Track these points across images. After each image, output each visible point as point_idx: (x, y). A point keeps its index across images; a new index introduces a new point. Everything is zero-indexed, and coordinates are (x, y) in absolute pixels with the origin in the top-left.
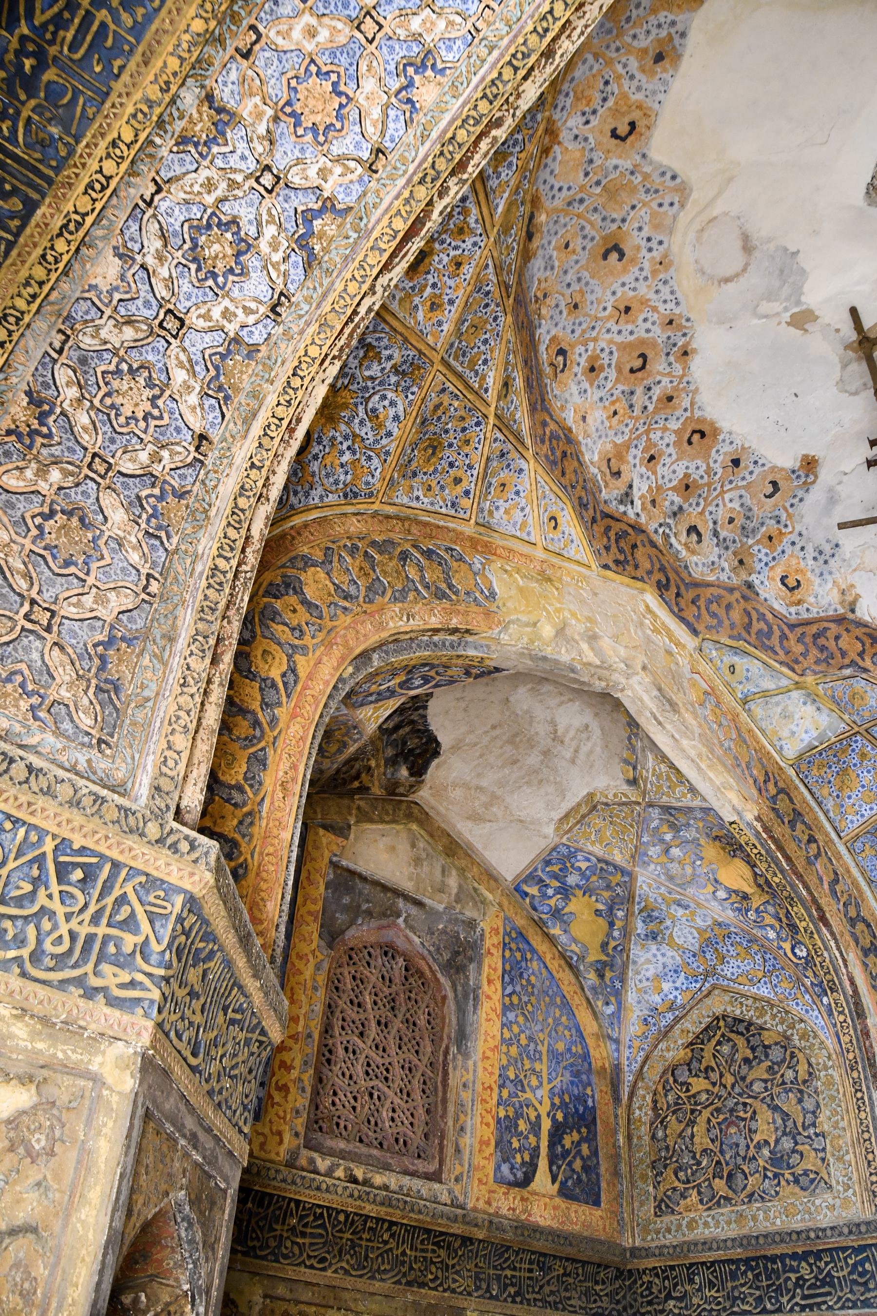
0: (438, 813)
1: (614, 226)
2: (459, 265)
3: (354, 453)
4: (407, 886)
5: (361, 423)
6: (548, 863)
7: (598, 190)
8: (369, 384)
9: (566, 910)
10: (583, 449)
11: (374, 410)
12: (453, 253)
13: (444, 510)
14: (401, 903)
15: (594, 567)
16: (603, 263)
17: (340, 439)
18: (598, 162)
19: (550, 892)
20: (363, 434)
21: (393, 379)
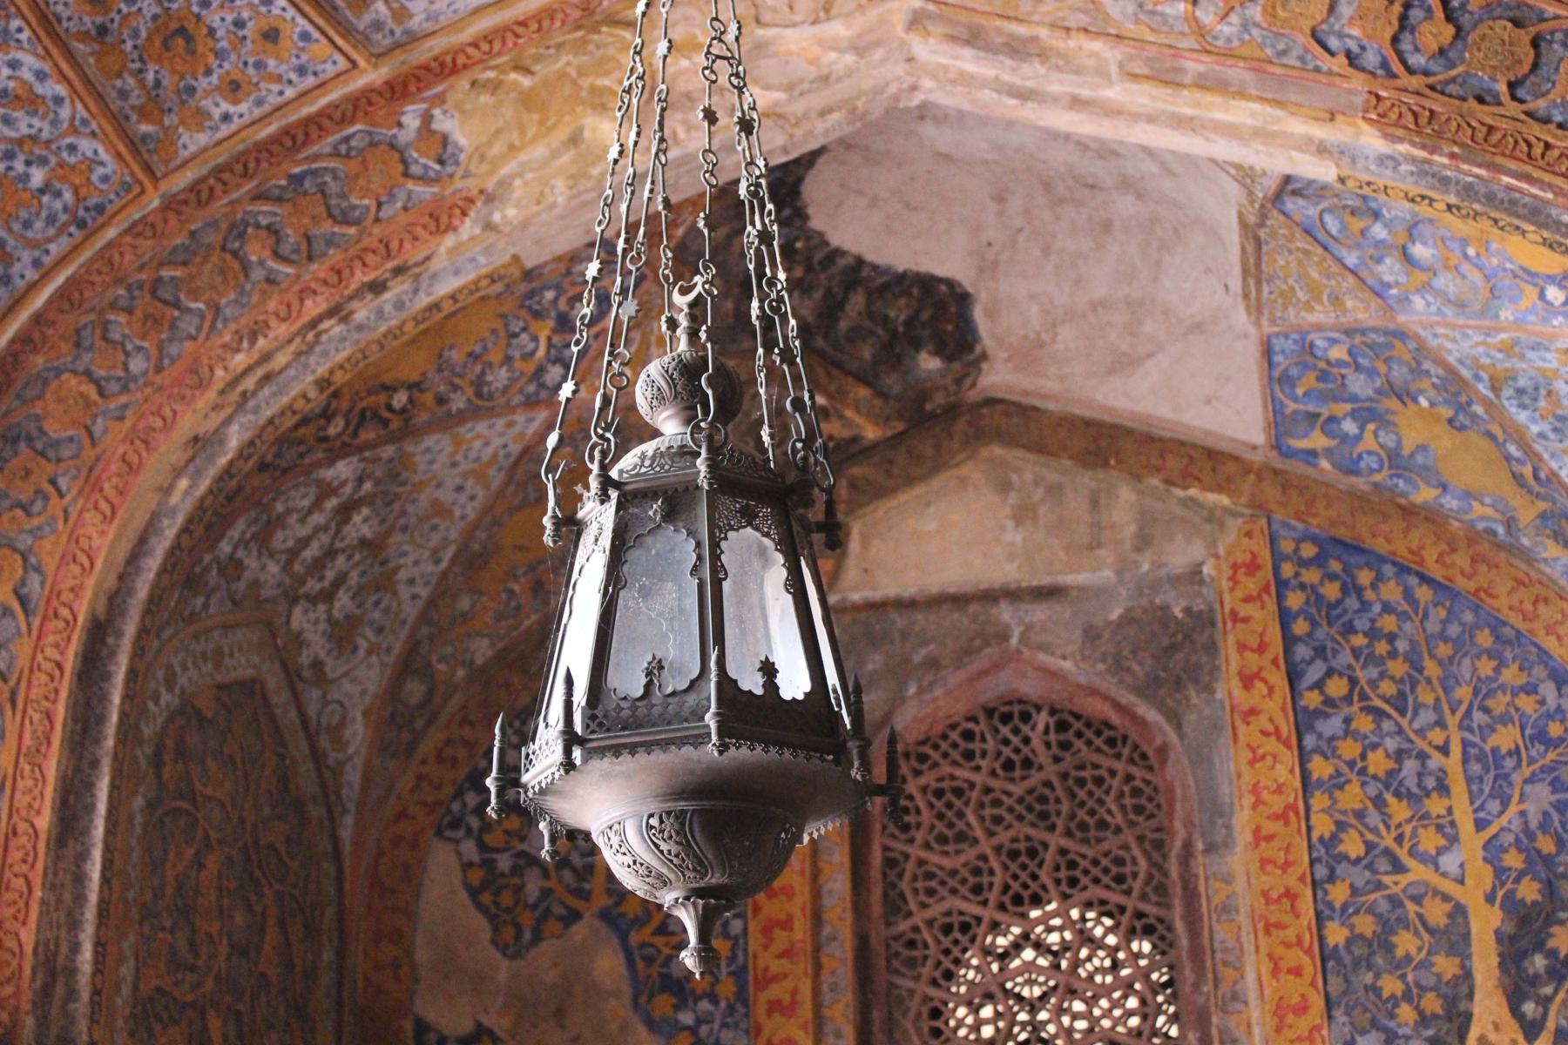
0: (1045, 397)
3: (43, 161)
4: (1008, 573)
6: (1286, 380)
9: (1406, 452)
13: (290, 93)
14: (1005, 612)
19: (1350, 427)
20: (25, 131)
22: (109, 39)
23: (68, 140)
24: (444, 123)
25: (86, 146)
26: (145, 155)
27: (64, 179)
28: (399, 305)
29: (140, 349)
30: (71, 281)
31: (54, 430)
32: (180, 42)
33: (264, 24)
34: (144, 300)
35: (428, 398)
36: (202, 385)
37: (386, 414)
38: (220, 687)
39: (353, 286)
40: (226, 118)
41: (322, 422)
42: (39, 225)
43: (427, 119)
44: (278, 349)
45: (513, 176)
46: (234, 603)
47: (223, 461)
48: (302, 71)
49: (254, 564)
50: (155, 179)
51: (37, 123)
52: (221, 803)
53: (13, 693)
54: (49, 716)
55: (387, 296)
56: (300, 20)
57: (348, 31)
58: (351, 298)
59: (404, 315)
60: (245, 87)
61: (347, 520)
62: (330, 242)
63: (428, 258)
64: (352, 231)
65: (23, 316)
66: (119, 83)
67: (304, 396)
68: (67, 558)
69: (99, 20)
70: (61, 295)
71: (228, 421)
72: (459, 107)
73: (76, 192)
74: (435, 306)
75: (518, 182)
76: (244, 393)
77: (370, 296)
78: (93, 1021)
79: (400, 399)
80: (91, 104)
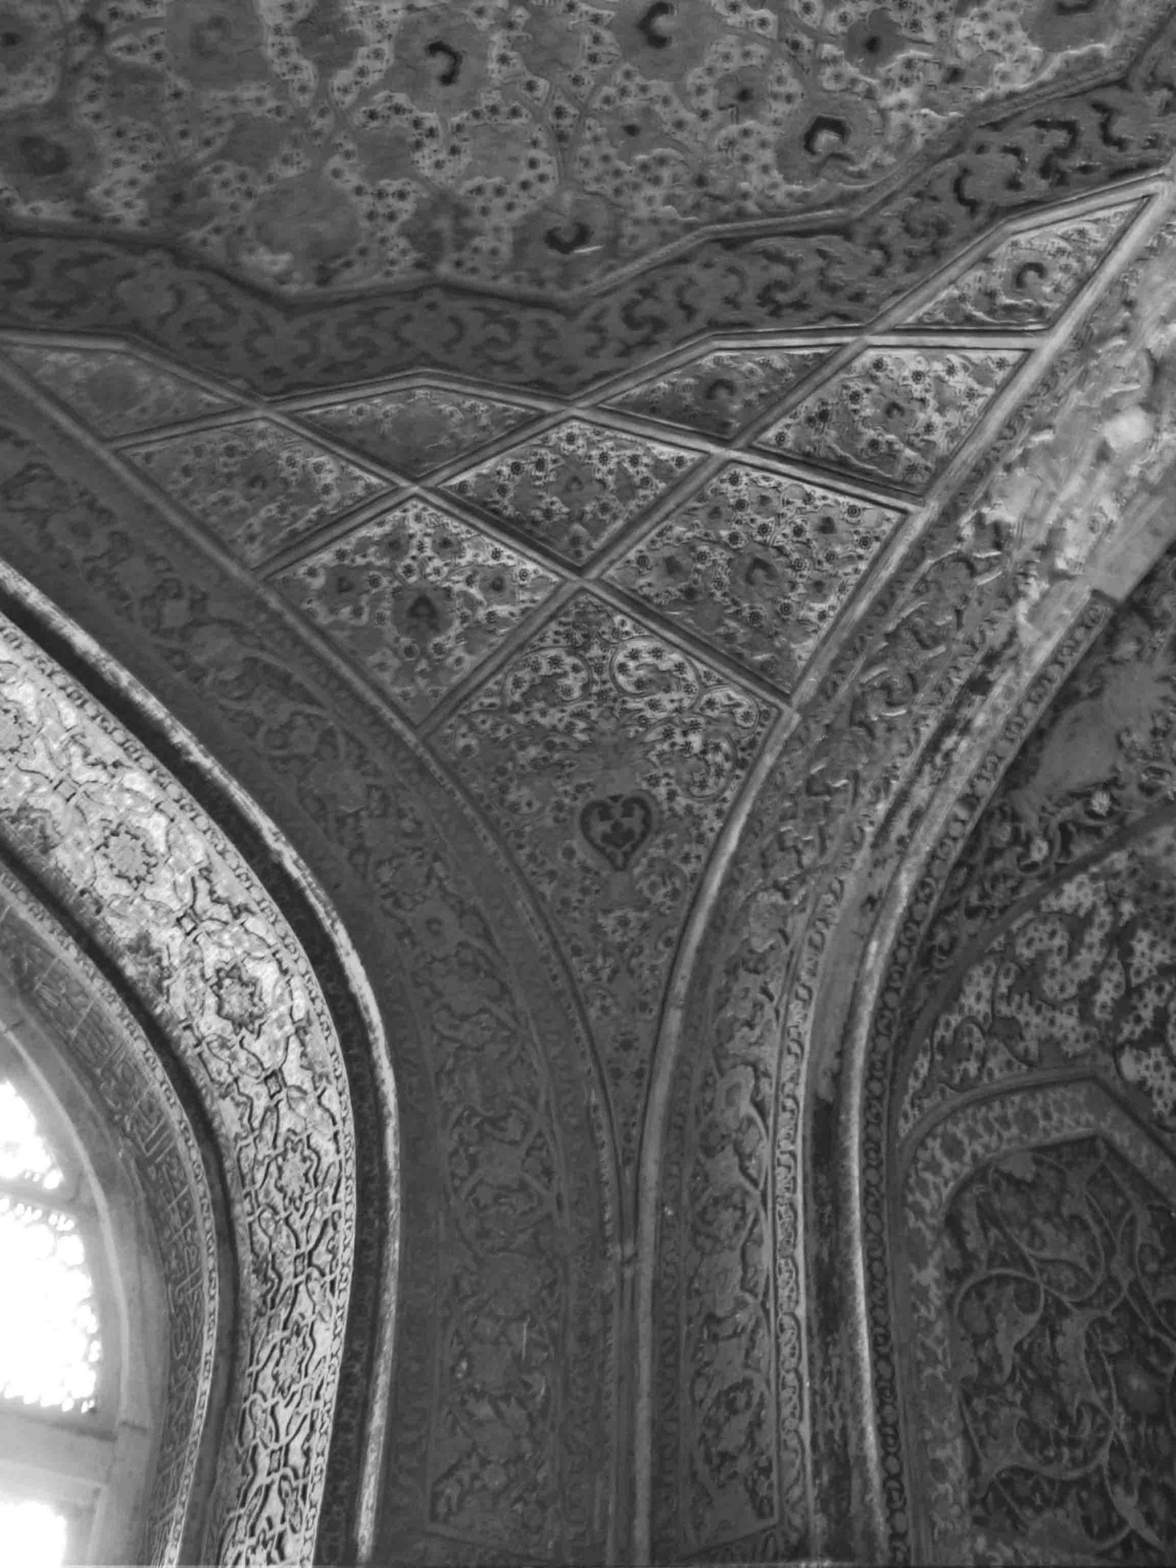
1: (607, 36)
2: (446, 543)
3: (694, 726)
5: (654, 705)
7: (542, 84)
8: (595, 689)
10: (1004, 88)
11: (639, 684)
12: (429, 552)
13: (863, 566)
15: (1150, 187)
16: (675, 45)
17: (666, 746)
18: (496, 97)
20: (671, 707)
21: (595, 651)
22: (700, 598)
23: (705, 698)
24: (992, 514)
25: (719, 695)
26: (768, 679)
27: (717, 733)
28: (1008, 693)
29: (807, 843)
30: (750, 816)
31: (760, 946)
32: (759, 574)
33: (815, 519)
34: (805, 801)
35: (1133, 791)
36: (857, 846)
37: (1091, 822)
38: (1041, 1149)
39: (954, 693)
40: (822, 616)
41: (1019, 849)
42: (711, 781)
43: (979, 520)
44: (911, 782)
45: (1061, 520)
46: (1031, 1065)
47: (900, 910)
48: (865, 543)
49: (1036, 1020)
50: (786, 698)
51: (675, 695)
52: (1075, 1268)
53: (764, 1195)
54: (792, 1206)
55: (997, 691)
56: (841, 499)
57: (884, 486)
58: (958, 705)
59: (1015, 699)
60: (827, 582)
61: (1130, 951)
62: (927, 668)
63: (1013, 634)
64: (942, 649)
65: (723, 862)
66: (721, 630)
67: (956, 819)
68: (784, 1051)
69: (683, 585)
70: (747, 830)
71: (896, 874)
72: (1003, 495)
73: (728, 737)
74: (1041, 679)
75: (1069, 524)
76: (901, 841)
77: (978, 698)
78: (892, 1512)
79: (1101, 802)
80: (705, 658)
